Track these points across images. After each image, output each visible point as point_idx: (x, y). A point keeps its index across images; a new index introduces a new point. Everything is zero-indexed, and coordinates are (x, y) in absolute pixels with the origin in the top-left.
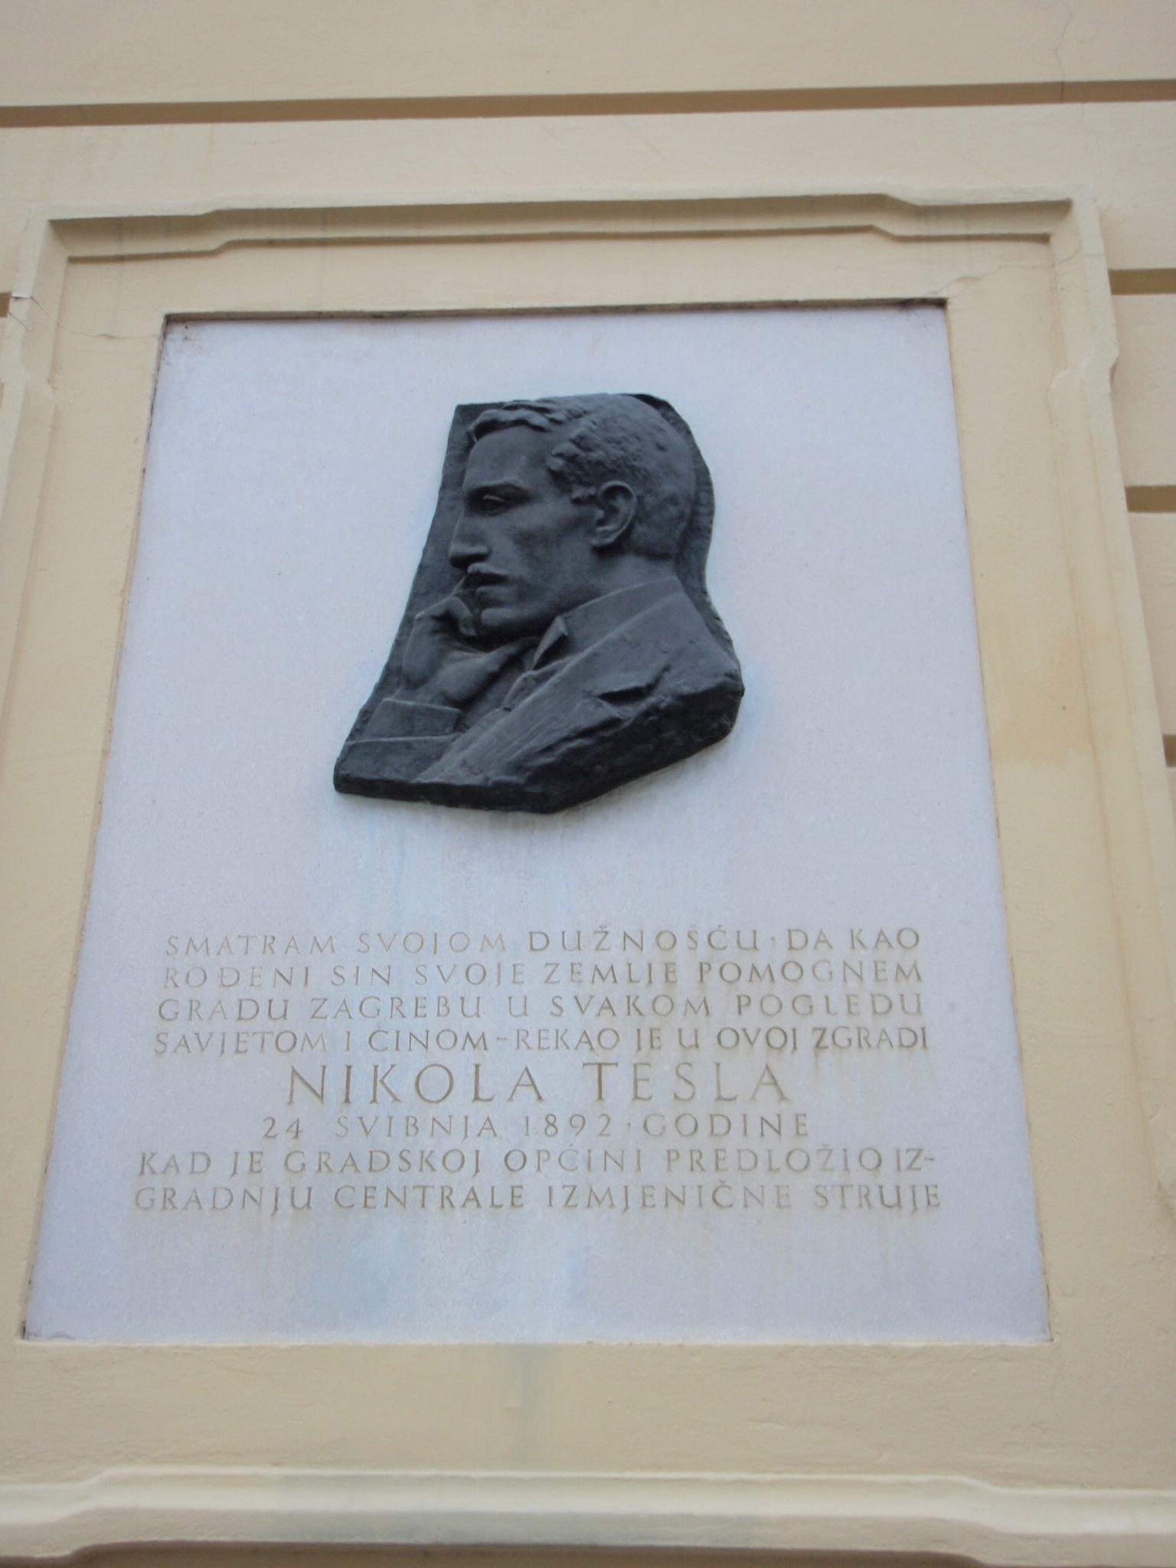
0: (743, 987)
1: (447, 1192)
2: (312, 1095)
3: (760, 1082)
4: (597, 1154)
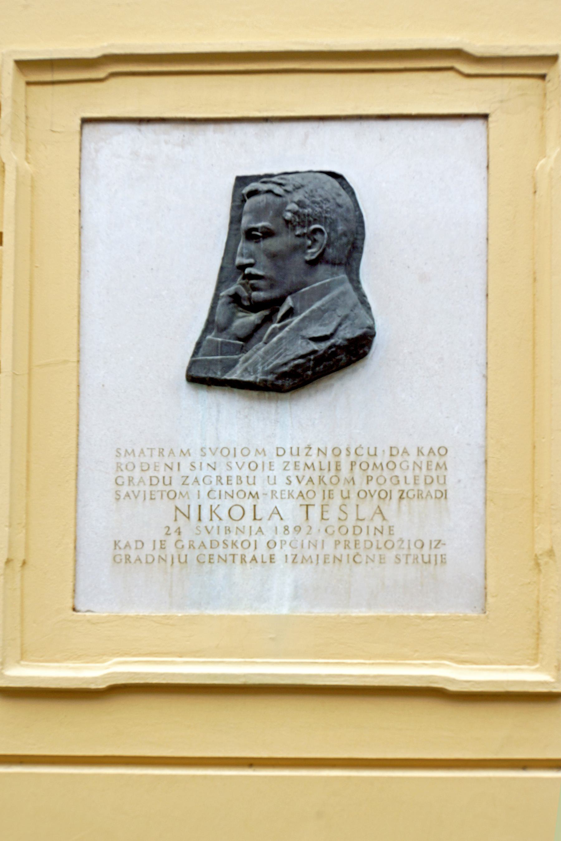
0: (370, 472)
1: (243, 557)
2: (184, 517)
3: (375, 513)
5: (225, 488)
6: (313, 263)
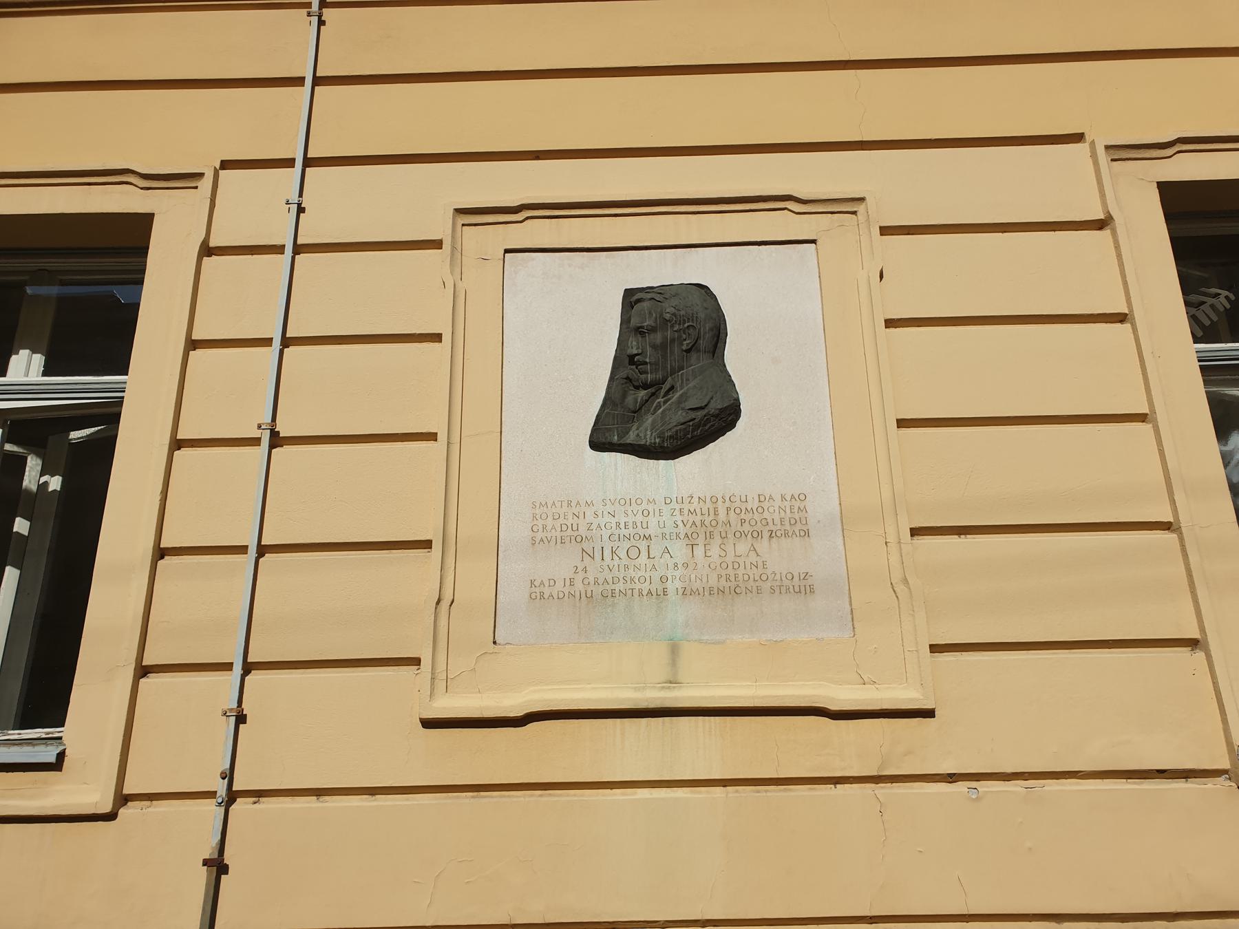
0: (743, 516)
4: (693, 577)
5: (624, 532)
6: (688, 351)
